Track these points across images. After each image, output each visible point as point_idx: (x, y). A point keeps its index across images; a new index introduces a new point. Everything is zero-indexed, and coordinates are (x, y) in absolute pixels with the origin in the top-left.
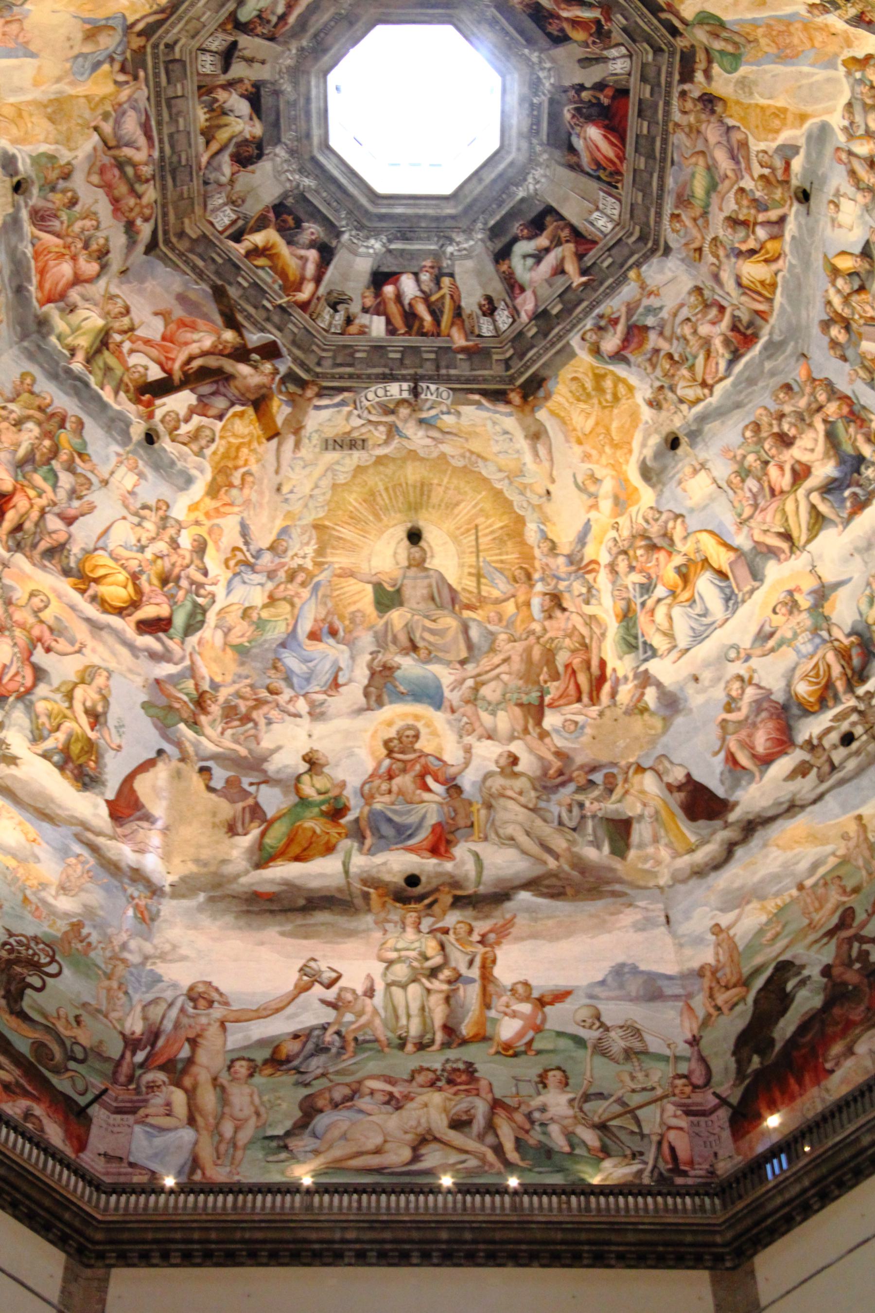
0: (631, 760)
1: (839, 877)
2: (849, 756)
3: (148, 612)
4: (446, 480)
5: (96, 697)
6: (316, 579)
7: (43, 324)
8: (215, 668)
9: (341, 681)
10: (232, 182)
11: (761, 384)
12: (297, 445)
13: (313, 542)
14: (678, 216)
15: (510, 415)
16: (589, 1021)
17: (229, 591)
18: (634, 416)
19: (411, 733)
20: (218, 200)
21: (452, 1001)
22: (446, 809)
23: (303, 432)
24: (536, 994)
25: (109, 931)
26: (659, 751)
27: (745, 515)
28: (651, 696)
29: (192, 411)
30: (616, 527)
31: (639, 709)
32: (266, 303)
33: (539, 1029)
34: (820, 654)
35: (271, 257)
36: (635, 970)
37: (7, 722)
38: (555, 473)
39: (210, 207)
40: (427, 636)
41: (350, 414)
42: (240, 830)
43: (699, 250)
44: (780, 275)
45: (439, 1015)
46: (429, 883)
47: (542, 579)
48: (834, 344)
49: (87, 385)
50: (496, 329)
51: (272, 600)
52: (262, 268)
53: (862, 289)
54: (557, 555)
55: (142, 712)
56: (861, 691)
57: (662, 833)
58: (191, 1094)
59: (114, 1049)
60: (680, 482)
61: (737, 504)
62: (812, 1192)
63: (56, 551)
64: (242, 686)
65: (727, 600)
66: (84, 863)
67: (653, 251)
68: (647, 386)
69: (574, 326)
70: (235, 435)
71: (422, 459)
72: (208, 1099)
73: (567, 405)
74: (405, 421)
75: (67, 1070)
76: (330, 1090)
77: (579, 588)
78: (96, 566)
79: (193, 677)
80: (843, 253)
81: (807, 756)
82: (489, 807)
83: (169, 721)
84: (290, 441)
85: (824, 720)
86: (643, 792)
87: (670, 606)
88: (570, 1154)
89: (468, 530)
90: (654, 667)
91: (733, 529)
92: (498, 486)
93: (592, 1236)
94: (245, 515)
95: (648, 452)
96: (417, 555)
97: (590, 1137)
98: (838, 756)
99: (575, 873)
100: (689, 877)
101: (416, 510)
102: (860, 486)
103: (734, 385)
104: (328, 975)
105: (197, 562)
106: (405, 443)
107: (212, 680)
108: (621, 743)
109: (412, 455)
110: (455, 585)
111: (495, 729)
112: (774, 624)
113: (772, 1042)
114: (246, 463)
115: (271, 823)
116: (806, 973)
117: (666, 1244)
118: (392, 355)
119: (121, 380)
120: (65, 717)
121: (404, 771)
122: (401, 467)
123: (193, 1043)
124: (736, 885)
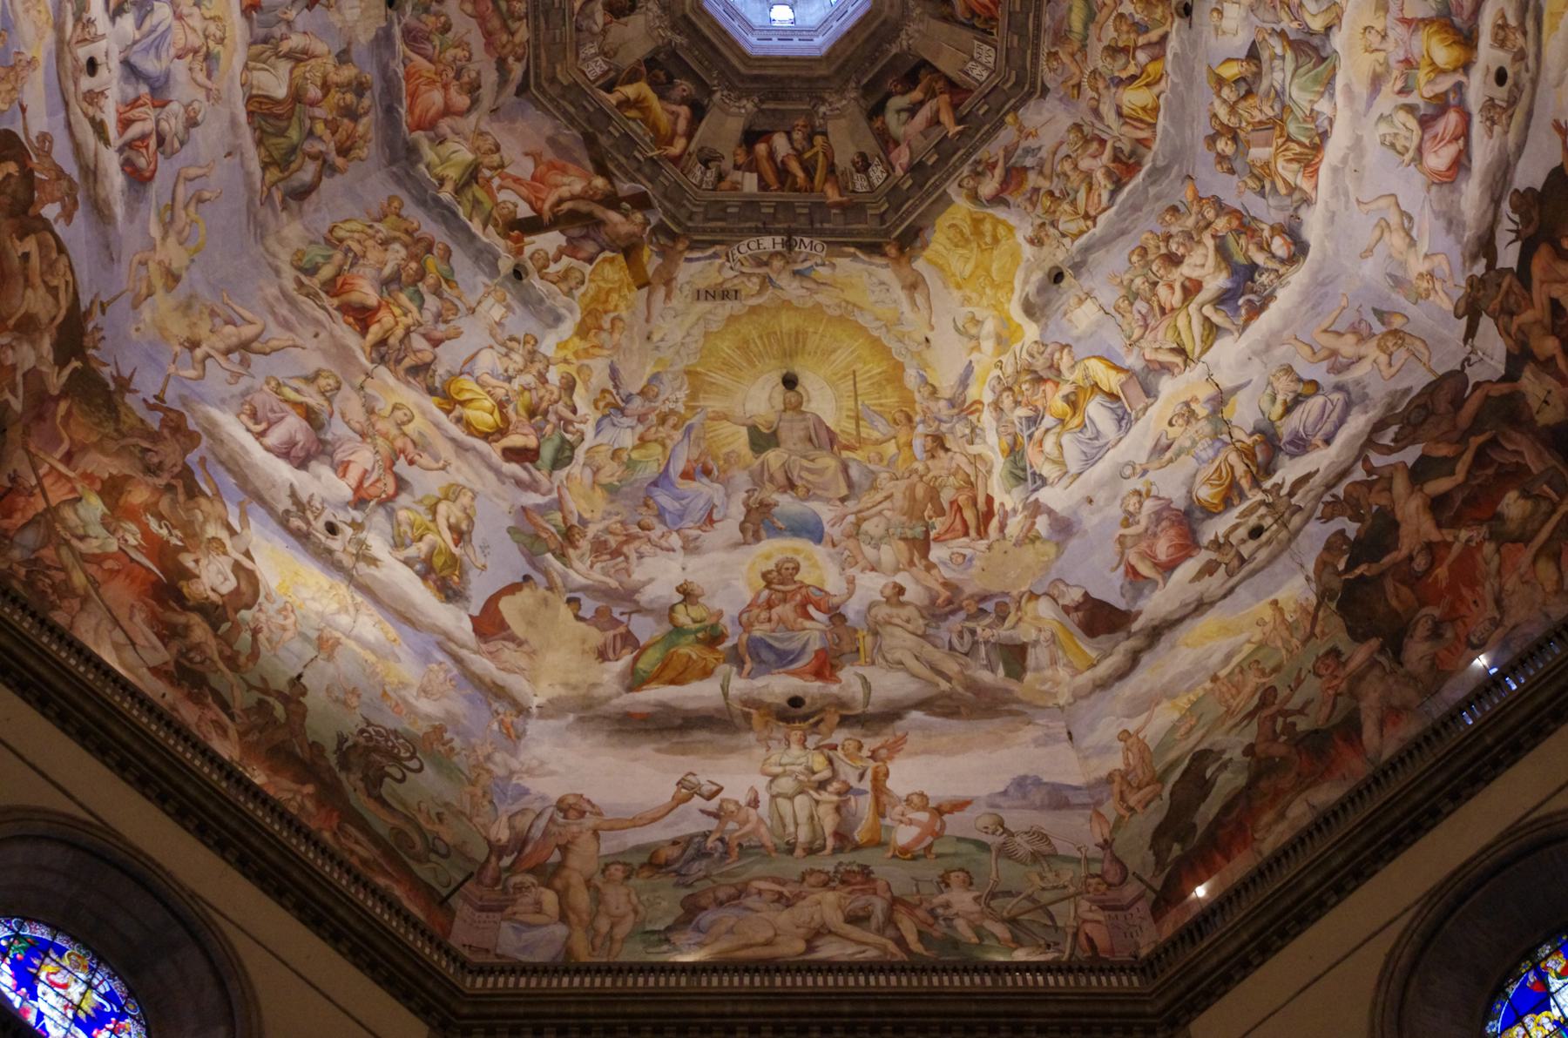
1: (1257, 662)
2: (1259, 547)
3: (515, 440)
5: (461, 515)
7: (412, 151)
8: (583, 504)
9: (715, 517)
10: (604, 32)
11: (1145, 209)
12: (668, 296)
14: (1056, 53)
15: (887, 266)
16: (992, 828)
17: (598, 431)
18: (1015, 255)
19: (791, 565)
20: (591, 49)
21: (844, 811)
24: (932, 804)
25: (473, 740)
26: (1053, 576)
27: (1135, 337)
28: (1042, 525)
30: (1000, 365)
31: (1030, 538)
32: (636, 154)
33: (938, 835)
34: (1221, 457)
35: (640, 109)
36: (1038, 782)
37: (367, 524)
39: (582, 56)
41: (722, 266)
42: (611, 655)
43: (1078, 86)
44: (1163, 97)
45: (829, 822)
47: (923, 422)
48: (1221, 158)
49: (455, 214)
50: (870, 184)
51: (643, 441)
52: (634, 120)
53: (1249, 93)
54: (938, 399)
56: (1268, 485)
57: (1060, 653)
58: (562, 895)
59: (480, 853)
60: (1065, 314)
61: (1125, 327)
62: (1253, 945)
63: (420, 370)
64: (613, 523)
65: (1120, 420)
66: (447, 671)
67: (1030, 95)
69: (950, 175)
70: (605, 280)
71: (797, 309)
72: (581, 899)
73: (945, 252)
74: (779, 273)
75: (429, 861)
76: (714, 890)
77: (962, 429)
78: (461, 390)
79: (561, 509)
80: (1229, 60)
81: (1212, 555)
82: (876, 634)
84: (661, 292)
85: (1232, 517)
86: (1037, 618)
87: (1059, 435)
88: (980, 945)
90: (1045, 496)
91: (1122, 351)
92: (876, 334)
93: (1010, 1008)
94: (615, 359)
95: (1031, 289)
97: (1000, 930)
98: (1245, 551)
99: (969, 694)
100: (1091, 693)
102: (1253, 292)
103: (1117, 213)
104: (707, 788)
105: (565, 398)
106: (779, 292)
108: (1012, 574)
109: (787, 304)
111: (879, 561)
112: (1171, 436)
113: (1194, 826)
115: (644, 650)
116: (1226, 756)
117: (1089, 1016)
118: (764, 210)
119: (490, 214)
120: (428, 529)
121: (785, 601)
123: (564, 849)
124: (1145, 688)
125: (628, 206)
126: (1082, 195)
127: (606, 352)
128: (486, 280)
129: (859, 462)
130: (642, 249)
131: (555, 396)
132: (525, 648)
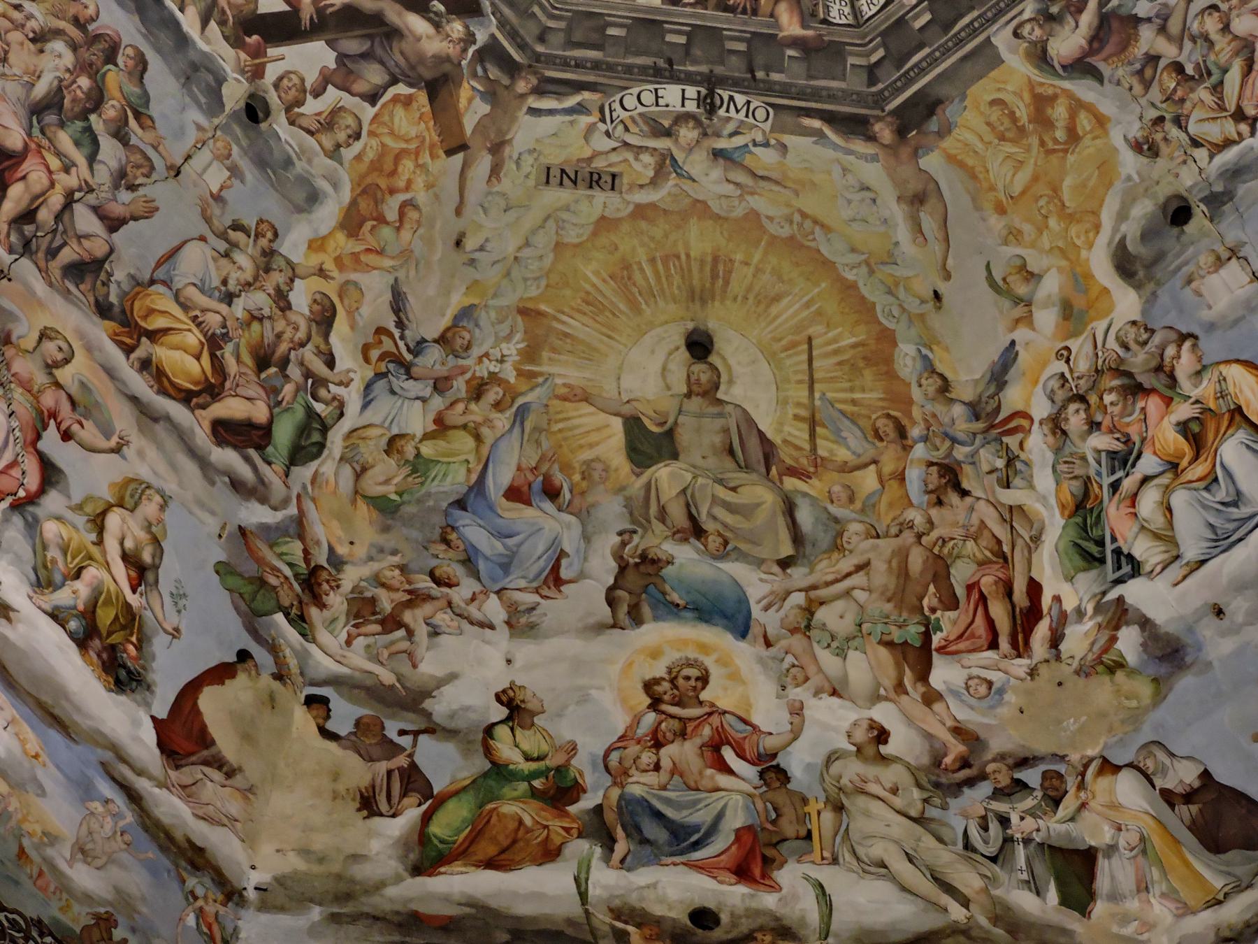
0: (1090, 752)
3: (231, 408)
4: (757, 257)
5: (142, 535)
6: (520, 401)
8: (337, 530)
9: (564, 574)
12: (495, 171)
13: (518, 336)
15: (874, 158)
18: (1106, 166)
19: (694, 672)
22: (760, 805)
23: (507, 151)
26: (1146, 735)
28: (1129, 642)
29: (326, 79)
30: (1065, 355)
38: (950, 262)
40: (720, 512)
42: (384, 807)
46: (734, 925)
47: (925, 439)
51: (442, 426)
54: (952, 400)
55: (216, 578)
57: (1156, 873)
64: (386, 566)
66: (117, 816)
68: (1135, 117)
70: (392, 133)
71: (717, 217)
73: (980, 146)
77: (990, 458)
78: (151, 312)
79: (301, 537)
82: (839, 808)
83: (259, 604)
84: (484, 163)
86: (1115, 806)
87: (1167, 490)
89: (794, 345)
90: (1135, 592)
92: (850, 276)
94: (401, 274)
95: (1131, 229)
96: (704, 378)
99: (999, 932)
101: (703, 302)
105: (317, 339)
106: (687, 185)
107: (331, 550)
108: (1071, 724)
109: (700, 208)
110: (769, 435)
111: (845, 679)
114: (408, 188)
118: (670, 38)
120: (91, 558)
121: (683, 735)
122: (678, 227)
125: (442, 8)
126: (1233, 77)
127: (388, 263)
128: (202, 119)
129: (814, 501)
130: (459, 85)
131: (301, 335)
132: (238, 780)
